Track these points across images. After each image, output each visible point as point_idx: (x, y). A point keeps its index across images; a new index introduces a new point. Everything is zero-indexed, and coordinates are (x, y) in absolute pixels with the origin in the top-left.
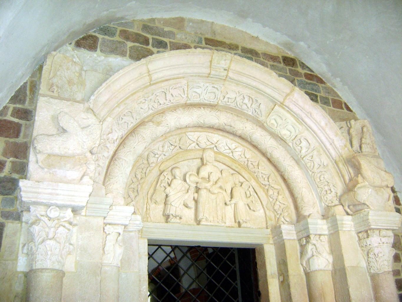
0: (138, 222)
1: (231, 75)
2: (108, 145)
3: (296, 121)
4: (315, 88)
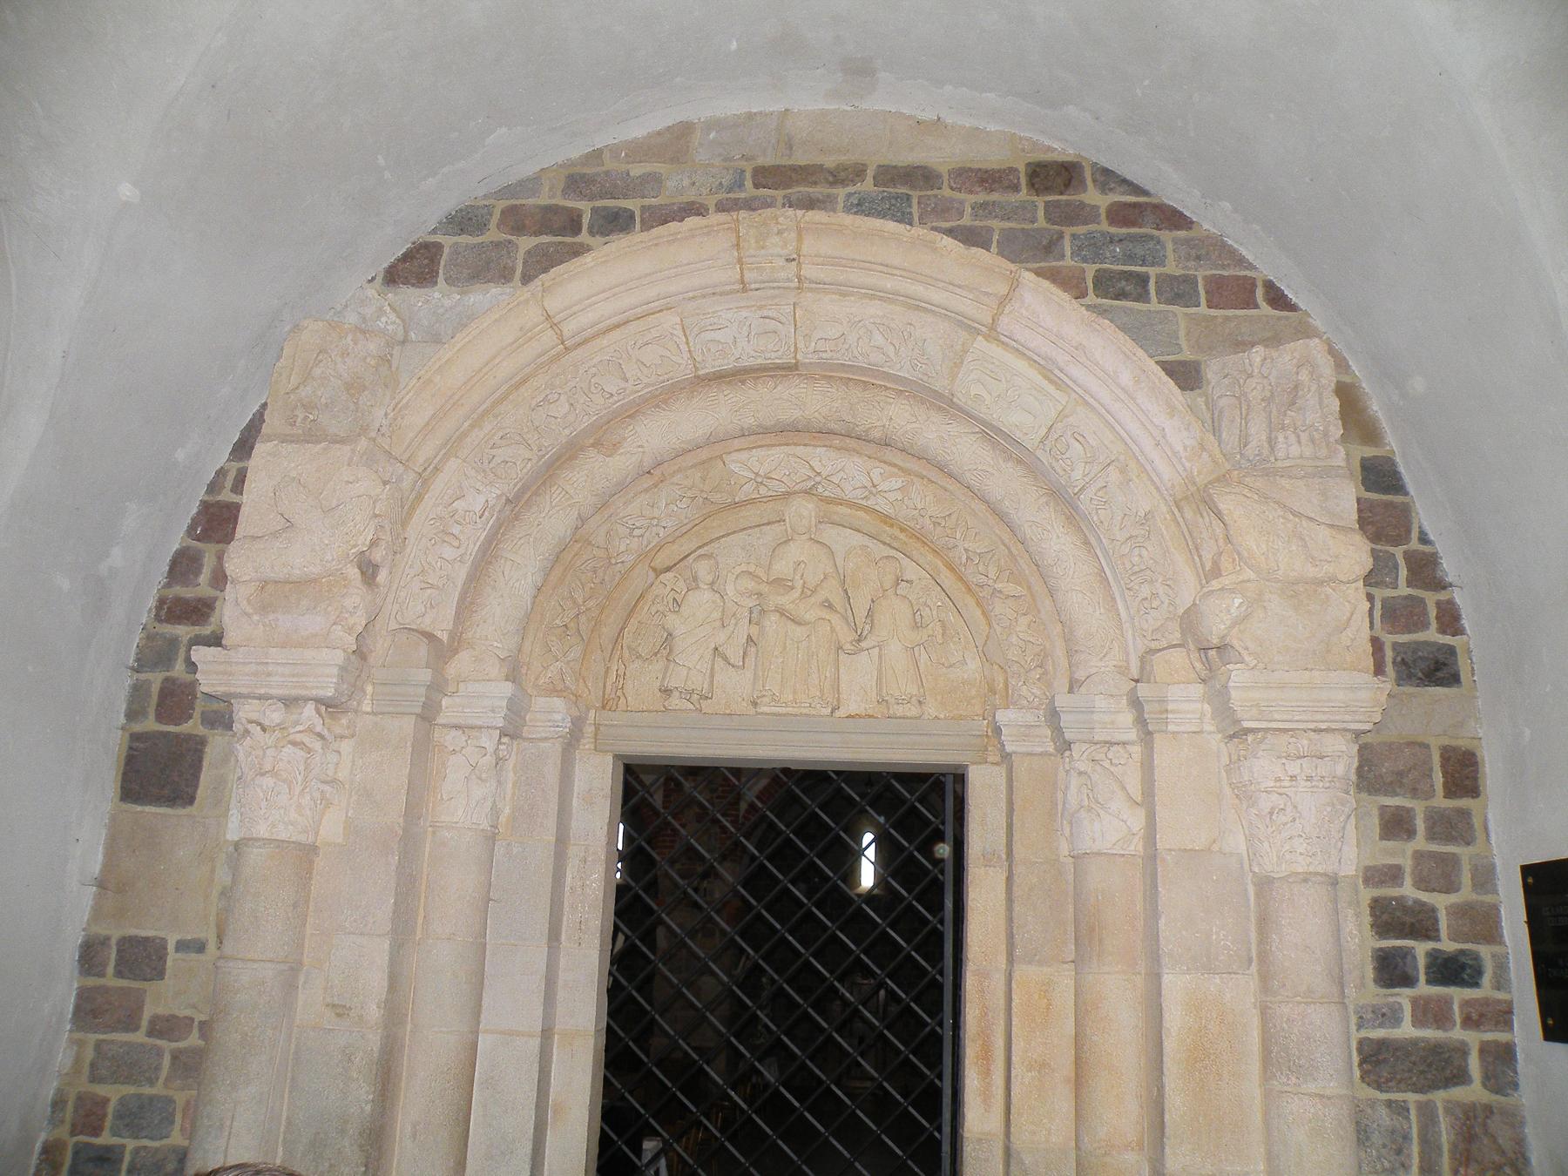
0: (558, 717)
1: (808, 271)
2: (456, 530)
3: (1045, 377)
4: (1139, 251)
